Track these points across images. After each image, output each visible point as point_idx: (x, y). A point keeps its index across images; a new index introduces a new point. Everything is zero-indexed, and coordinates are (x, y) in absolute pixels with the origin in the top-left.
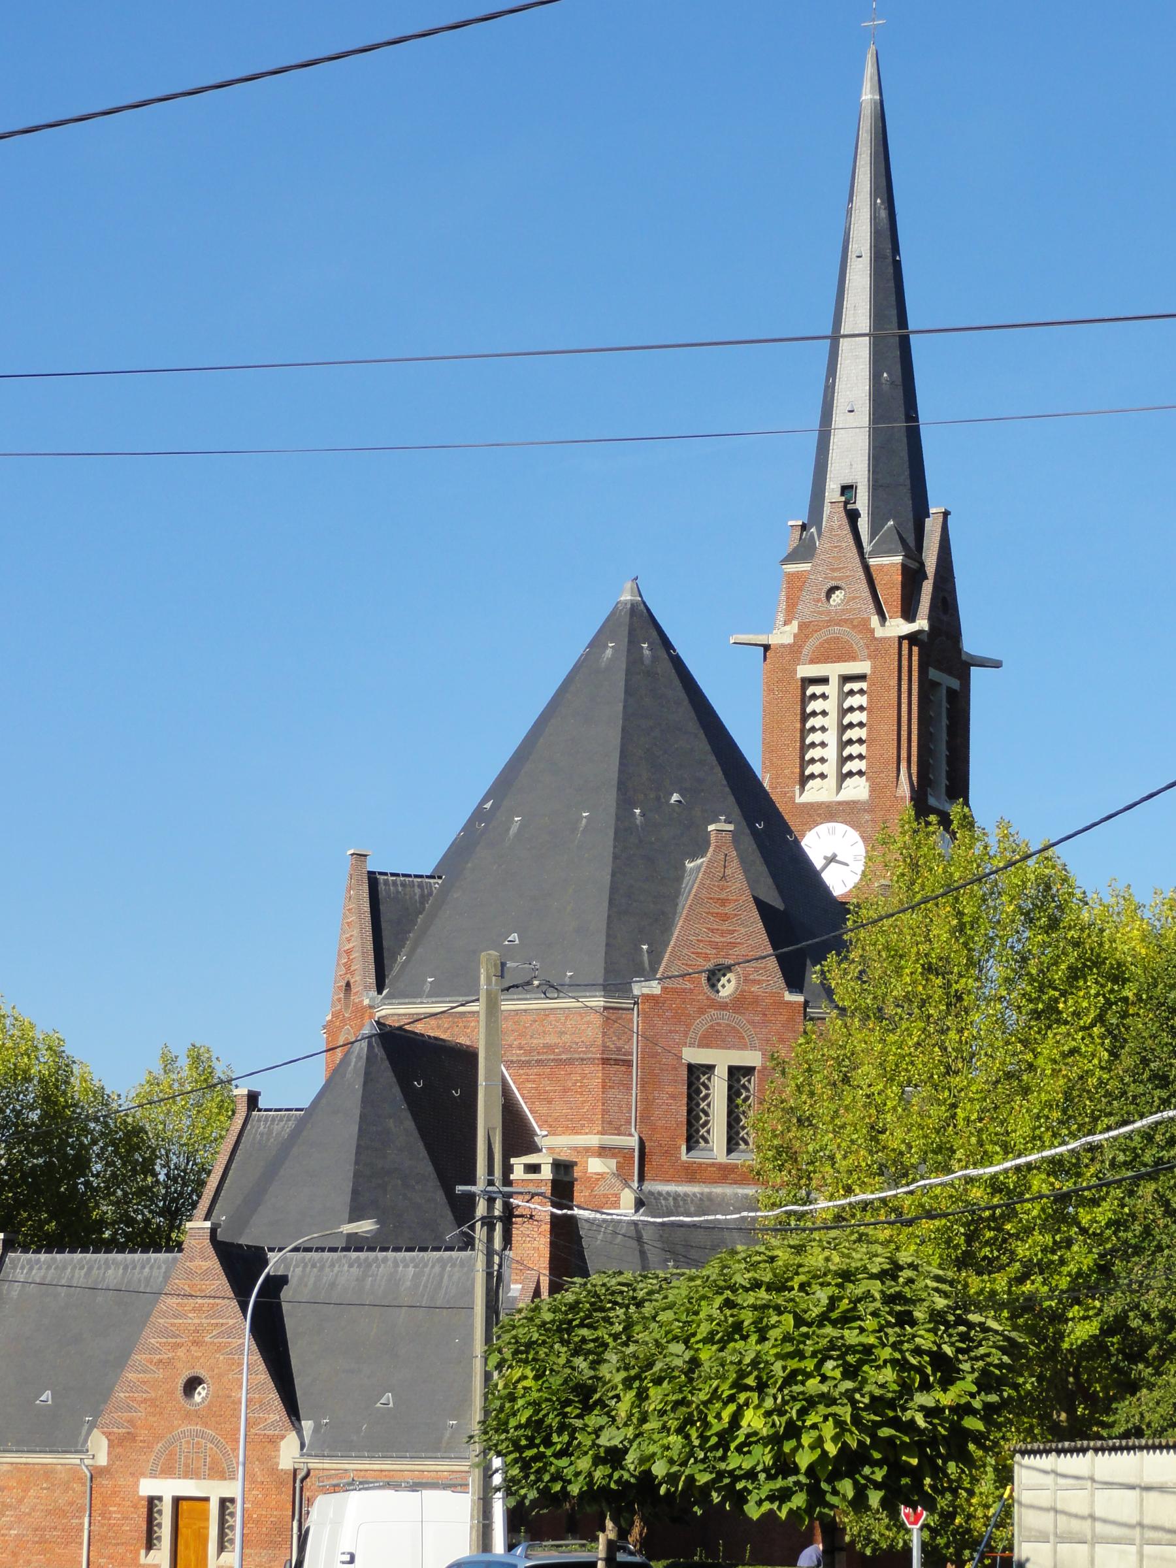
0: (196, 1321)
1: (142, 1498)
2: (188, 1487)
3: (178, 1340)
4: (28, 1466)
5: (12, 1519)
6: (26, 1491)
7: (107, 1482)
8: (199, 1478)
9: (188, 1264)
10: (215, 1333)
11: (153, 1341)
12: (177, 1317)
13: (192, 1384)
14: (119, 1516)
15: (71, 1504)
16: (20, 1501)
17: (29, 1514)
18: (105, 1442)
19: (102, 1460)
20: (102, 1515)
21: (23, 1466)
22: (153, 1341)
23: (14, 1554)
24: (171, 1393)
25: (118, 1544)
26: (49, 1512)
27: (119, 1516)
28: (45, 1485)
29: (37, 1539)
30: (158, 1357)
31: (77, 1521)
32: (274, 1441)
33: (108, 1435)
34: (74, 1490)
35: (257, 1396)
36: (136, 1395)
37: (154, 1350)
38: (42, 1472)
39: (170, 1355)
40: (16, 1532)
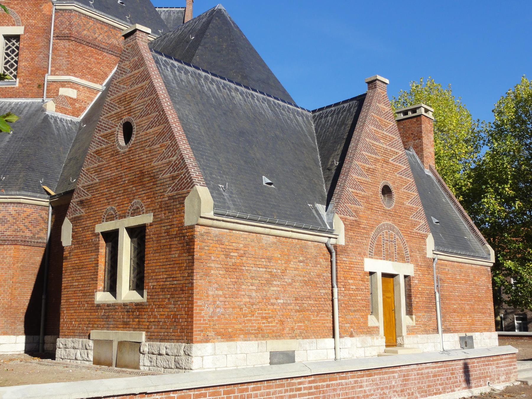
0: (385, 146)
1: (366, 273)
2: (389, 267)
3: (377, 157)
4: (288, 240)
5: (279, 289)
6: (288, 261)
7: (346, 259)
8: (393, 261)
9: (378, 104)
10: (394, 157)
11: (364, 152)
12: (375, 140)
13: (386, 191)
14: (354, 287)
15: (319, 276)
16: (284, 272)
17: (290, 284)
18: (342, 226)
19: (342, 241)
20: (344, 286)
21: (284, 239)
22: (364, 152)
23: (282, 322)
24: (376, 194)
25: (355, 311)
26: (306, 283)
27: (354, 287)
28: (301, 258)
29: (298, 308)
30: (368, 166)
31: (324, 291)
32: (424, 238)
33: (344, 220)
34: (320, 264)
35: (415, 206)
36: (358, 192)
37: (366, 161)
38: (298, 246)
39: (374, 166)
40: (282, 301)
